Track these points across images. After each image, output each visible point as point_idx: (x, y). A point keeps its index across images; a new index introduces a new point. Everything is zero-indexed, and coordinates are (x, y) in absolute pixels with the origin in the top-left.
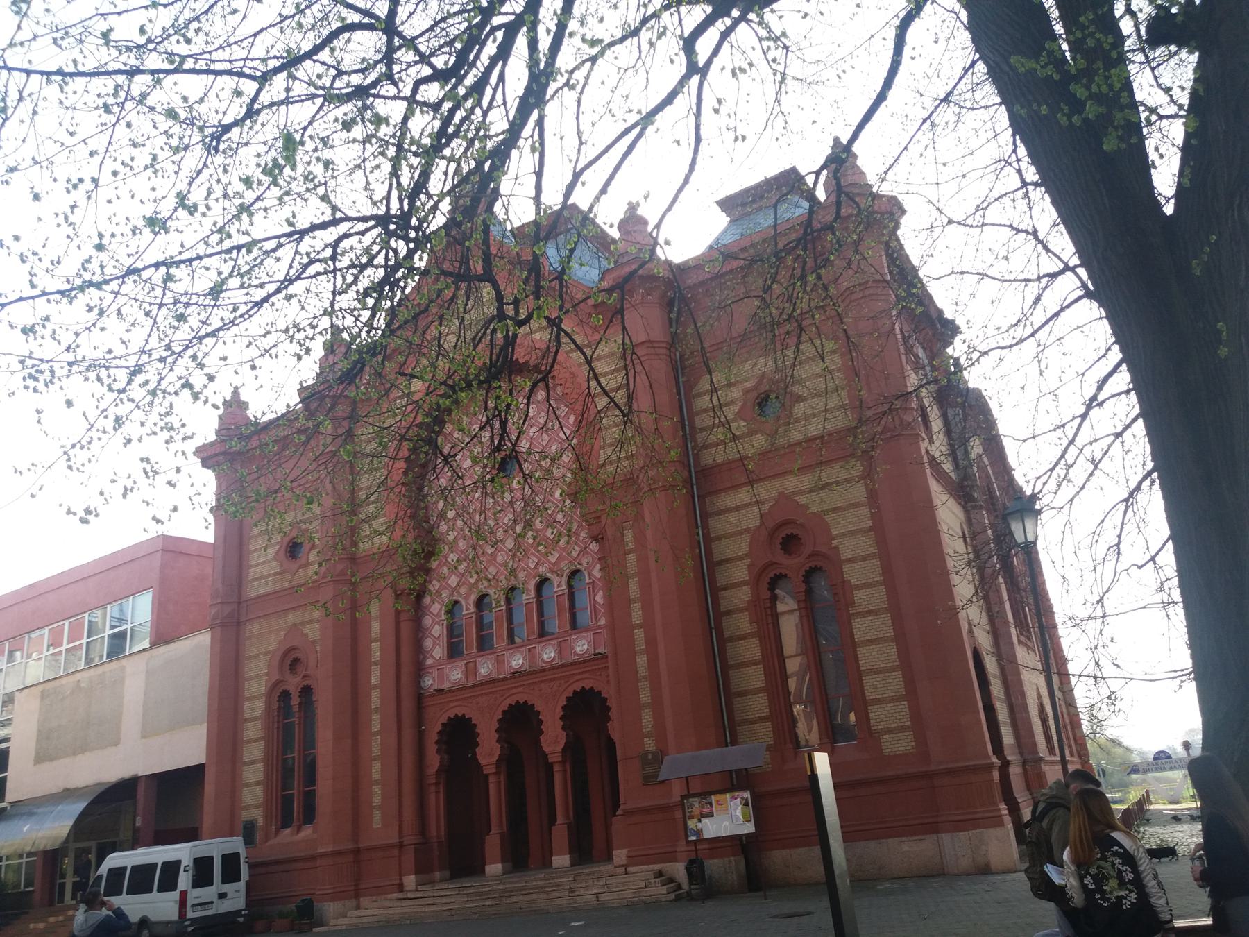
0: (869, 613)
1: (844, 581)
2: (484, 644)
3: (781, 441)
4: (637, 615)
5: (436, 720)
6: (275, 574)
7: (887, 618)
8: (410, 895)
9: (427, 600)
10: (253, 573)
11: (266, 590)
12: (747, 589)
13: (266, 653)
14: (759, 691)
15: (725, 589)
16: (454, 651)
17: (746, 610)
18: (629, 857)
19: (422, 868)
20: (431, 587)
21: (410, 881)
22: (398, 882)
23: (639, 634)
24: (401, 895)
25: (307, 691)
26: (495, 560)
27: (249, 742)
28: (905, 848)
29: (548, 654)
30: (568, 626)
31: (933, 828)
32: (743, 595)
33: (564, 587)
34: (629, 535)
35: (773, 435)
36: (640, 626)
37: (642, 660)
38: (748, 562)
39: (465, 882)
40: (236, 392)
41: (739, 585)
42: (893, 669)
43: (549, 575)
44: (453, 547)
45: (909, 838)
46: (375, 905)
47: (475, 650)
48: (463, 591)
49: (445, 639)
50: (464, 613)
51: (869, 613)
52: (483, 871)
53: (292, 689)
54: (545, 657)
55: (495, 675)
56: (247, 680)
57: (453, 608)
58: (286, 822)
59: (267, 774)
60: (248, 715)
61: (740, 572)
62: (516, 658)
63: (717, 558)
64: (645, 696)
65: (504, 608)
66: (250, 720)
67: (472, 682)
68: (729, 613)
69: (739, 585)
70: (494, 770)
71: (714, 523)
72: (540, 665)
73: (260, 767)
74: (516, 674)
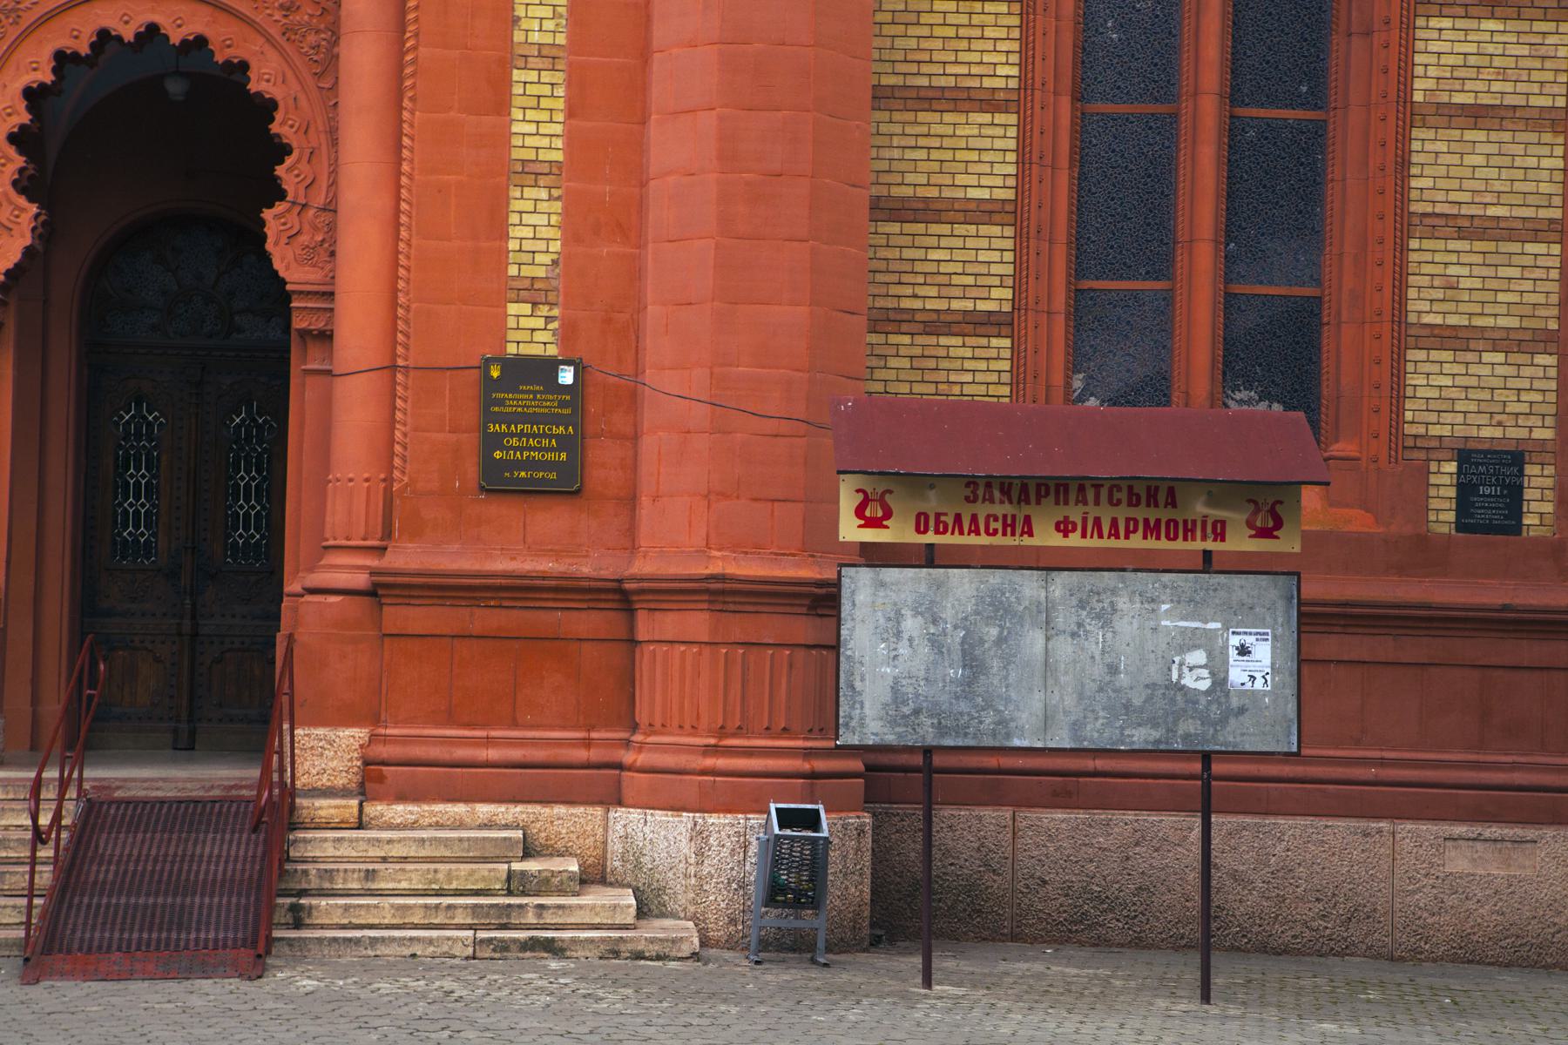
14: (983, 213)
28: (1459, 862)
42: (1535, 231)
45: (1476, 829)
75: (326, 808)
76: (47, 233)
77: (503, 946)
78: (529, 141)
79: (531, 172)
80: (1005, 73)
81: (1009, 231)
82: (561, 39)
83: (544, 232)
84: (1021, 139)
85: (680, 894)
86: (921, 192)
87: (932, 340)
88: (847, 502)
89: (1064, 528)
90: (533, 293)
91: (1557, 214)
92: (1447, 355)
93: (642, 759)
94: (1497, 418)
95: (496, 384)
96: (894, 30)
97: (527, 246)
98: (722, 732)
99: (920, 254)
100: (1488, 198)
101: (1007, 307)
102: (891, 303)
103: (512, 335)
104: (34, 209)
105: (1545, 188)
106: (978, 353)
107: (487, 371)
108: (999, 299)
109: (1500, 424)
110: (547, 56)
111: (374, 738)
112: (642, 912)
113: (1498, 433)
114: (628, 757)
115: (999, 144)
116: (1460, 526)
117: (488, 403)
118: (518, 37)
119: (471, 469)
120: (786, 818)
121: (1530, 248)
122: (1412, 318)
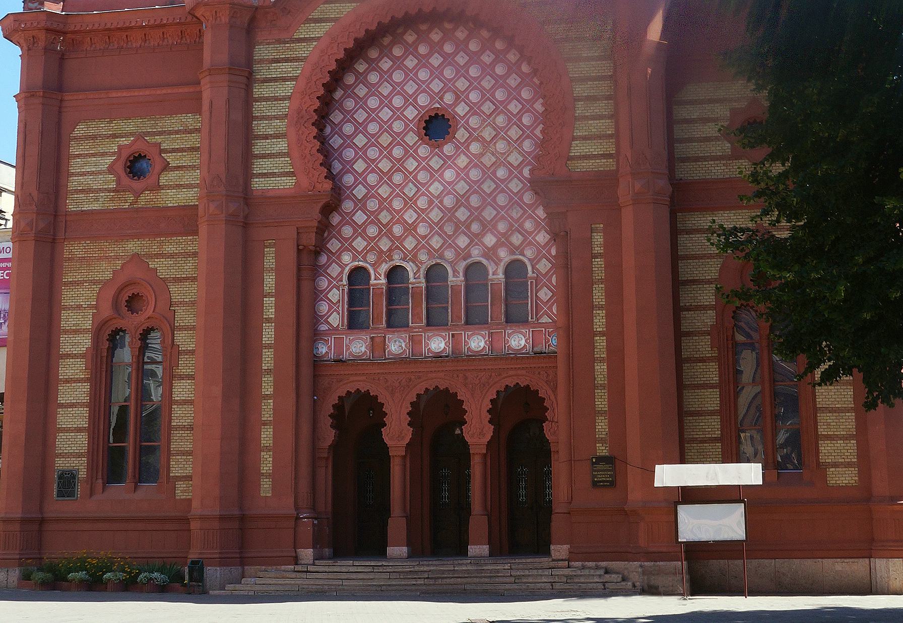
4: (599, 321)
6: (109, 191)
9: (323, 259)
11: (96, 206)
12: (712, 313)
13: (95, 282)
14: (712, 413)
15: (689, 309)
17: (709, 334)
23: (601, 343)
26: (415, 229)
32: (708, 319)
34: (598, 239)
36: (602, 334)
37: (601, 369)
41: (705, 308)
43: (484, 261)
44: (361, 204)
47: (384, 324)
48: (371, 258)
49: (346, 306)
50: (372, 281)
63: (682, 277)
64: (602, 402)
65: (424, 285)
66: (68, 356)
68: (689, 334)
69: (705, 308)
71: (683, 239)
74: (438, 356)
78: (599, 406)
79: (601, 413)
80: (716, 379)
81: (719, 417)
82: (606, 382)
83: (604, 427)
84: (720, 395)
86: (697, 409)
87: (702, 445)
90: (602, 441)
91: (853, 406)
92: (829, 442)
94: (842, 457)
95: (595, 463)
96: (688, 371)
97: (601, 430)
99: (698, 424)
100: (835, 403)
101: (719, 436)
102: (691, 437)
103: (598, 451)
104: (493, 427)
105: (849, 399)
106: (713, 447)
107: (592, 460)
109: (843, 458)
110: (603, 386)
113: (843, 460)
115: (715, 396)
118: (596, 382)
121: (847, 414)
122: (819, 433)
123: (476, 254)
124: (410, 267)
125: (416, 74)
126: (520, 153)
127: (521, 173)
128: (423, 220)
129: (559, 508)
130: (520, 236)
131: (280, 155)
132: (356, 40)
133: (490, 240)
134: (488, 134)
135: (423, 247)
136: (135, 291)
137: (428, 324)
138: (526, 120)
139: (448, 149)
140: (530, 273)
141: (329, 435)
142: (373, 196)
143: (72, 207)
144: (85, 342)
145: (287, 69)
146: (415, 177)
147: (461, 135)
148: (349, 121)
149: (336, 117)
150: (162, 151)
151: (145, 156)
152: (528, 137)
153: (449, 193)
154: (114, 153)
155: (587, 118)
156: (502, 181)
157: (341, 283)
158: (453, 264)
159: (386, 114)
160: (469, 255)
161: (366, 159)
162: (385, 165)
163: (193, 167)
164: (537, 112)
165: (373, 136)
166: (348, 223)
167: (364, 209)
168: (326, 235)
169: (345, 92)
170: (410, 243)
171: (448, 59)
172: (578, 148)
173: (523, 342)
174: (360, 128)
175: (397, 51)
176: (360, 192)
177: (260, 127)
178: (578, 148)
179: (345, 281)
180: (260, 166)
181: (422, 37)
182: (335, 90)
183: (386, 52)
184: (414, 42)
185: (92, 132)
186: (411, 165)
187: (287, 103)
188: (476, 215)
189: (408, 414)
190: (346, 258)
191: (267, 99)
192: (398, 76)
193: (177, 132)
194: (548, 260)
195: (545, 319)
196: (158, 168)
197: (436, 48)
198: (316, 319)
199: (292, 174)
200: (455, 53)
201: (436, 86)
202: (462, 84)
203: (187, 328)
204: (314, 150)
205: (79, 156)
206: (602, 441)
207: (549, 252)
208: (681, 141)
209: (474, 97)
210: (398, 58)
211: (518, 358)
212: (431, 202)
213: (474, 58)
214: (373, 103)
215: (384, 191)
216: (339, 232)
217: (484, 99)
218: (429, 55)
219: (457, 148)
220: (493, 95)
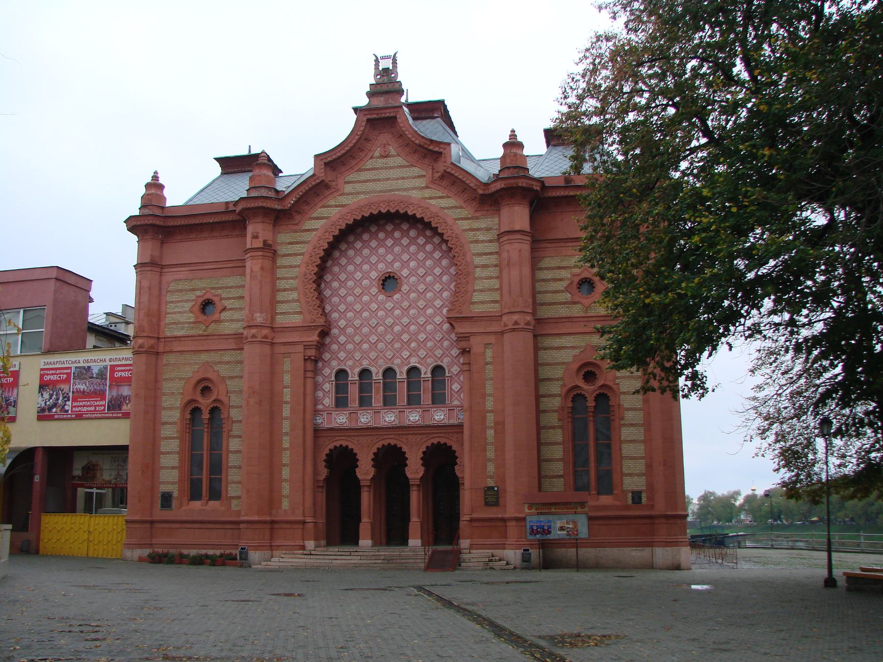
0: (632, 425)
1: (619, 405)
2: (364, 402)
3: (592, 313)
5: (328, 445)
6: (190, 323)
7: (642, 430)
8: (313, 552)
9: (320, 364)
10: (169, 319)
12: (559, 399)
13: (181, 379)
15: (544, 396)
16: (341, 402)
17: (556, 411)
18: (471, 544)
19: (316, 539)
20: (323, 357)
21: (310, 544)
22: (302, 544)
24: (305, 552)
25: (214, 411)
26: (376, 347)
27: (166, 438)
28: (634, 553)
29: (414, 417)
30: (430, 403)
31: (650, 544)
32: (556, 402)
33: (429, 375)
34: (489, 353)
35: (587, 308)
37: (490, 433)
38: (561, 383)
39: (347, 549)
40: (155, 177)
42: (641, 458)
44: (343, 330)
46: (290, 556)
48: (350, 363)
51: (632, 425)
52: (356, 543)
53: (202, 408)
54: (411, 419)
55: (372, 424)
56: (165, 394)
57: (341, 374)
58: (195, 494)
59: (181, 461)
60: (164, 419)
61: (555, 388)
62: (389, 415)
63: (541, 377)
64: (490, 453)
65: (381, 381)
66: (166, 423)
67: (354, 426)
68: (544, 411)
70: (369, 484)
71: (541, 353)
72: (407, 423)
73: (177, 457)
75: (465, 551)
76: (426, 472)
77: (486, 568)
79: (490, 460)
85: (512, 562)
88: (526, 506)
89: (556, 509)
90: (491, 477)
93: (508, 543)
98: (518, 538)
104: (424, 468)
108: (561, 473)
110: (492, 443)
111: (472, 541)
112: (508, 564)
114: (506, 543)
116: (632, 503)
117: (485, 493)
119: (483, 503)
120: (525, 550)
123: (414, 362)
124: (373, 370)
125: (377, 252)
126: (441, 300)
127: (441, 312)
128: (381, 341)
129: (465, 517)
130: (441, 352)
131: (293, 301)
132: (340, 230)
133: (422, 353)
134: (421, 287)
135: (381, 358)
136: (206, 384)
137: (385, 404)
138: (445, 278)
139: (397, 296)
140: (447, 375)
141: (324, 473)
142: (350, 326)
143: (168, 334)
144: (175, 415)
145: (298, 248)
146: (376, 315)
147: (405, 288)
148: (335, 280)
149: (328, 277)
150: (221, 299)
151: (212, 302)
152: (446, 290)
153: (397, 324)
154: (193, 300)
155: (482, 278)
156: (430, 317)
157: (330, 379)
158: (400, 367)
159: (358, 275)
160: (409, 363)
161: (345, 303)
162: (358, 307)
163: (241, 309)
164: (452, 274)
165: (350, 289)
166: (335, 343)
167: (345, 334)
168: (321, 350)
169: (333, 263)
170: (373, 355)
171: (397, 242)
172: (477, 297)
173: (442, 417)
174: (343, 283)
175: (366, 236)
176: (342, 323)
177: (281, 284)
178: (477, 297)
179: (333, 379)
180: (281, 308)
181: (381, 228)
182: (327, 261)
183: (359, 237)
184: (377, 230)
185: (180, 287)
186: (374, 306)
187: (297, 269)
188: (414, 337)
189: (372, 460)
190: (334, 363)
191: (285, 267)
192: (366, 252)
193: (231, 287)
194: (457, 365)
195: (456, 403)
196: (220, 308)
197: (389, 234)
198: (316, 401)
199: (300, 313)
200: (402, 237)
201: (390, 258)
202: (405, 257)
203: (237, 407)
204: (314, 298)
205: (172, 302)
206: (491, 477)
207: (459, 361)
208: (540, 293)
209: (413, 264)
210: (366, 241)
211: (439, 426)
212: (386, 330)
213: (413, 241)
214: (351, 268)
215: (357, 323)
216: (329, 348)
217: (419, 266)
218: (386, 239)
219: (402, 297)
220: (424, 264)
